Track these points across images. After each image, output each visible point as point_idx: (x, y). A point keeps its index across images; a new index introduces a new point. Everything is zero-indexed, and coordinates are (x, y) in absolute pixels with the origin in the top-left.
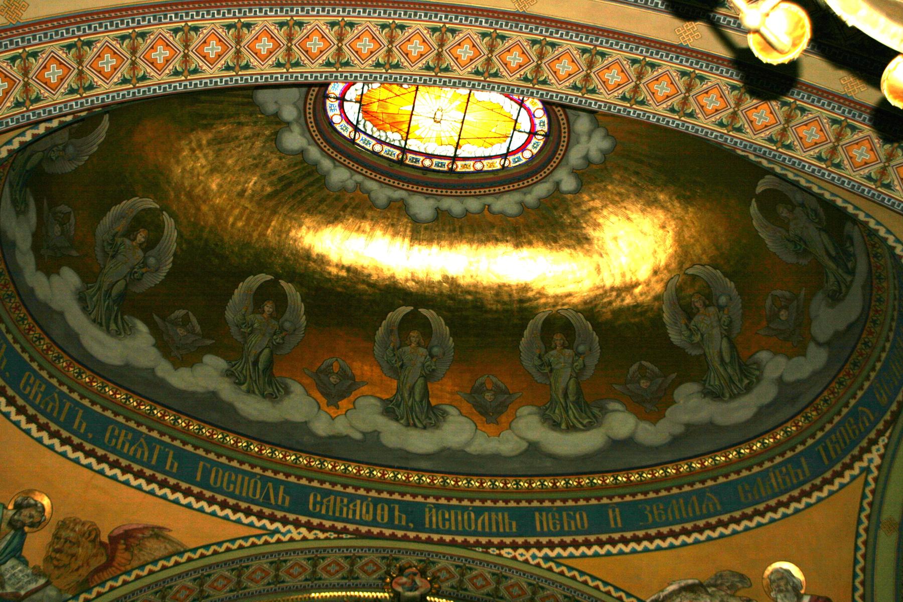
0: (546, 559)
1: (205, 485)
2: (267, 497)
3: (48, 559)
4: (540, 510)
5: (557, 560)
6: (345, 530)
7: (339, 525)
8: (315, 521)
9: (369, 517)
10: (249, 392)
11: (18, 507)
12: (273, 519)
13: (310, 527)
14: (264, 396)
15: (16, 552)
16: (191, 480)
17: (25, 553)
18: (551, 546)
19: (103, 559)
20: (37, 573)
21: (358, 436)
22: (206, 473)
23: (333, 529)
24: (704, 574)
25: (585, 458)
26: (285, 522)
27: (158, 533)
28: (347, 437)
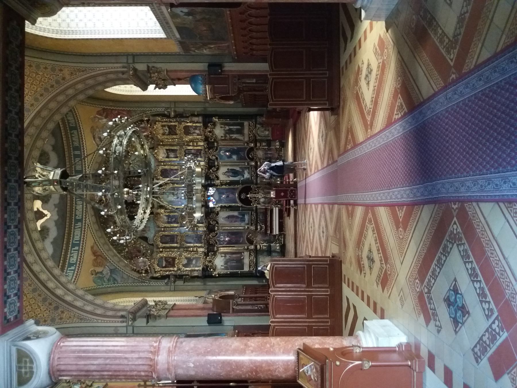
0: (88, 168)
1: (80, 241)
2: (80, 227)
3: (101, 267)
4: (75, 168)
5: (88, 166)
6: (86, 211)
7: (84, 212)
8: (84, 217)
9: (81, 206)
10: (48, 235)
11: (92, 275)
12: (85, 226)
13: (86, 218)
14: (48, 232)
15: (101, 273)
16: (79, 244)
17: (101, 271)
18: (85, 167)
19: (100, 257)
20: (105, 267)
21: (57, 209)
22: (76, 241)
23: (85, 213)
24: (91, 136)
25: (59, 157)
26: (85, 223)
27: (92, 248)
28: (57, 211)
